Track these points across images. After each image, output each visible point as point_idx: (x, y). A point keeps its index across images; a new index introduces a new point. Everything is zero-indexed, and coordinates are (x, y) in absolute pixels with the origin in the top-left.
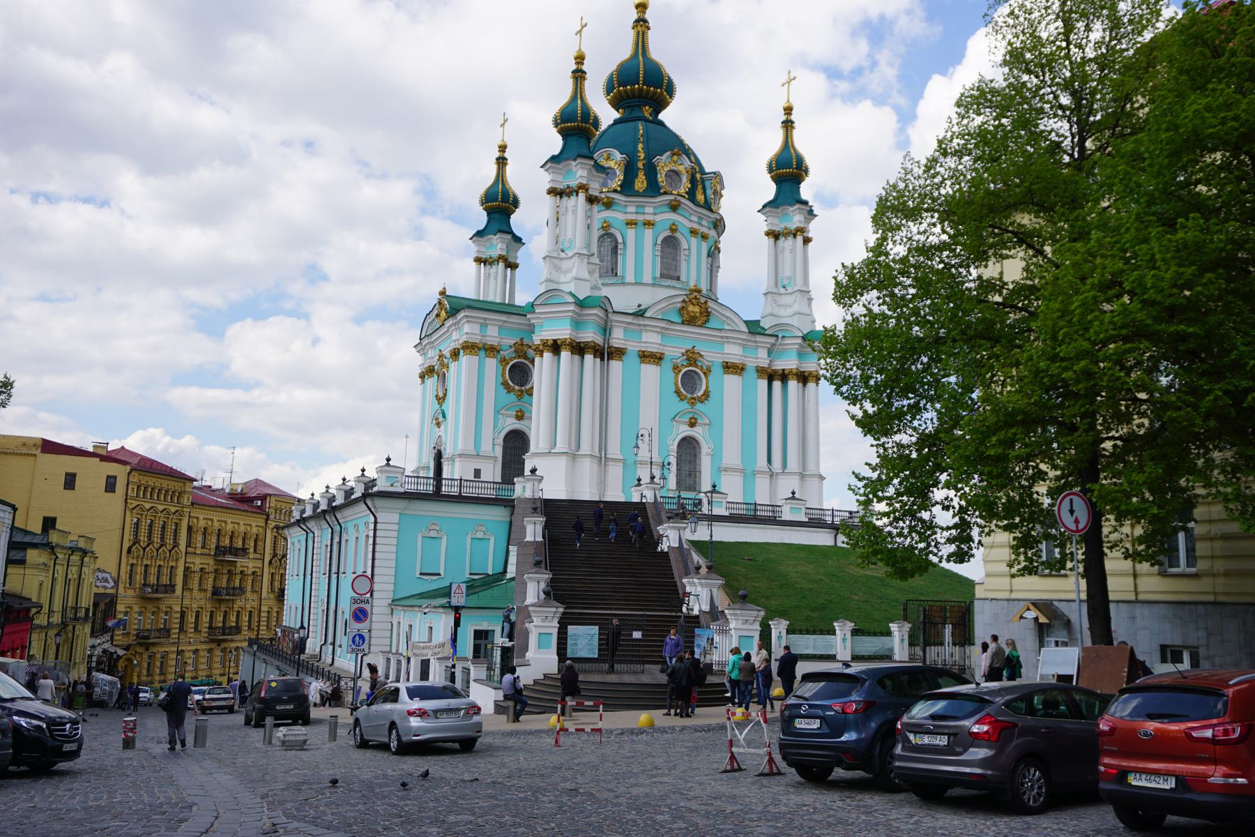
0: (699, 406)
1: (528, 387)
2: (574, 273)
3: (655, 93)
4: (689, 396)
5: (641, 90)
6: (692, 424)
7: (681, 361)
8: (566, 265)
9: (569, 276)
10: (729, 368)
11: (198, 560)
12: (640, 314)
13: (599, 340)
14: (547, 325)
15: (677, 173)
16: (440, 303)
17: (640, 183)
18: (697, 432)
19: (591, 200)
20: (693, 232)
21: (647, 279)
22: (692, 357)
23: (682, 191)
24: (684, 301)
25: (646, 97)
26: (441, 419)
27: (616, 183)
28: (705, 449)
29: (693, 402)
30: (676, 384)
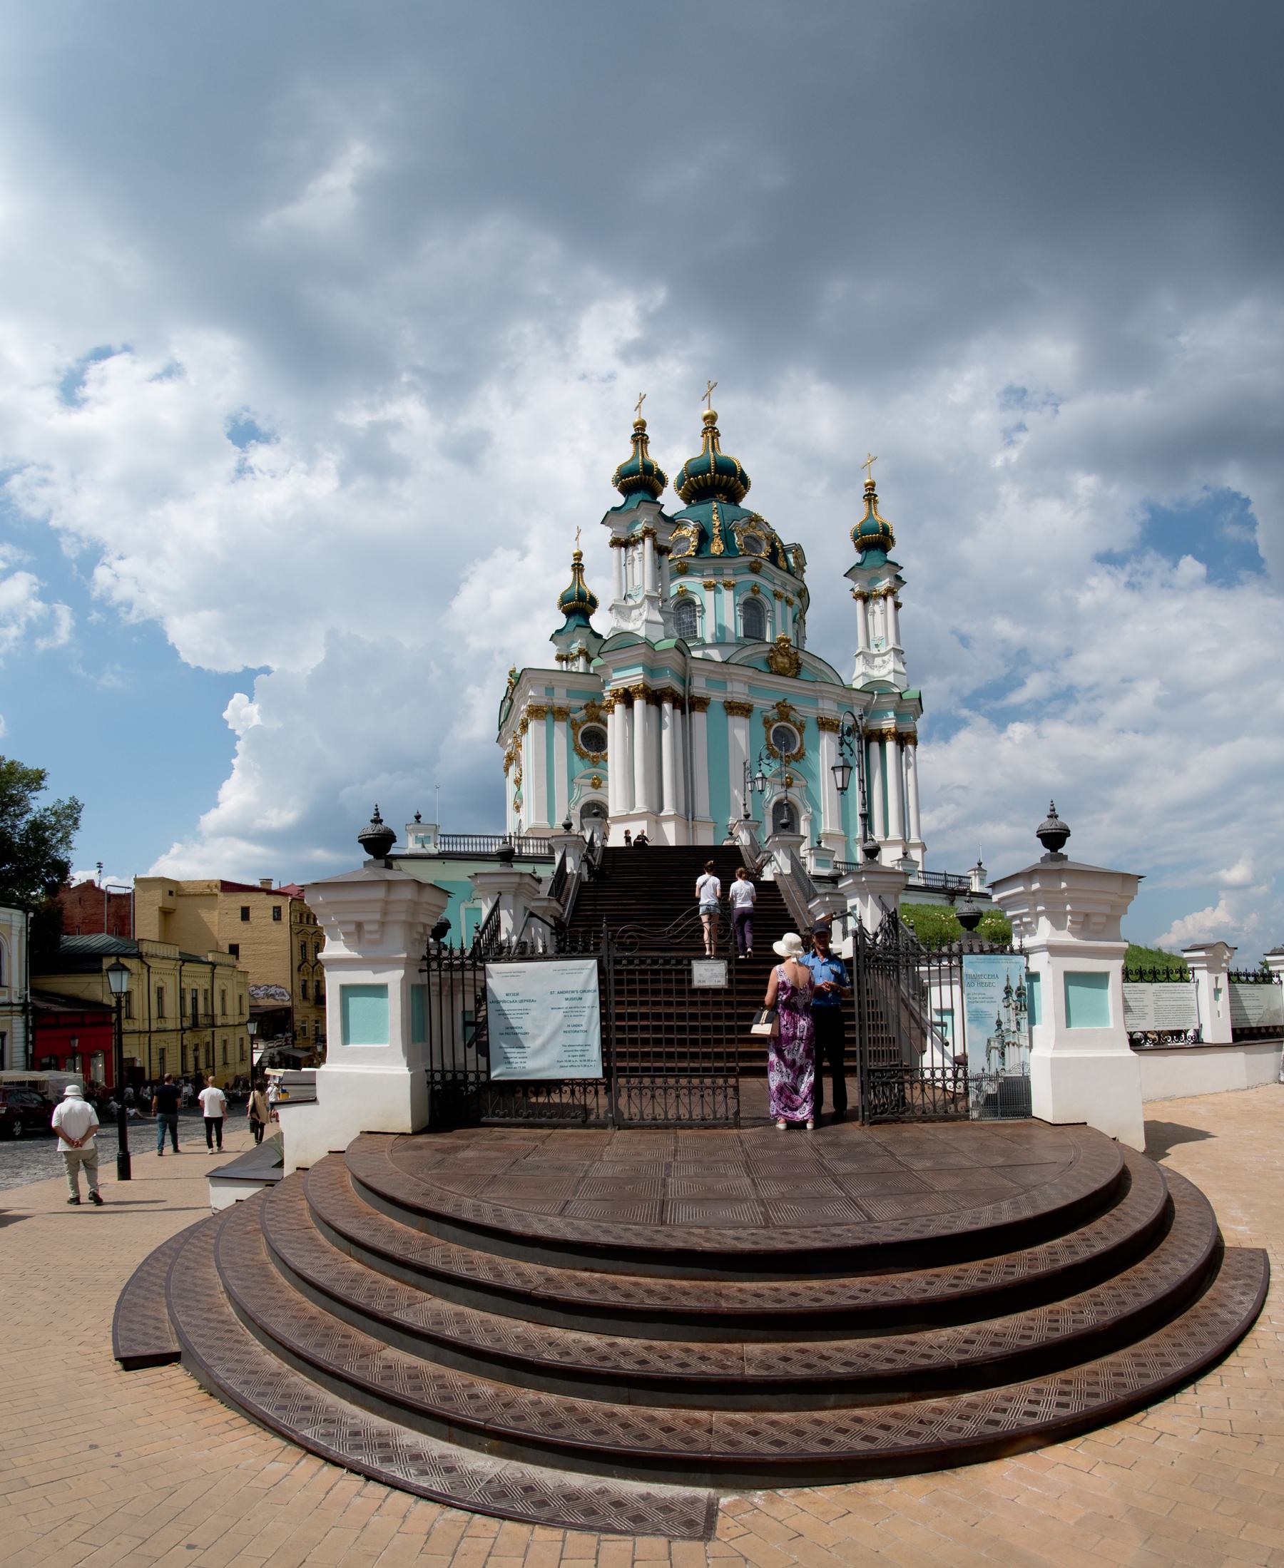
0: (793, 764)
2: (644, 617)
3: (728, 482)
5: (713, 478)
7: (772, 714)
8: (635, 613)
9: (639, 624)
10: (825, 725)
13: (678, 688)
14: (616, 676)
15: (756, 540)
17: (716, 547)
20: (777, 595)
22: (784, 710)
23: (763, 554)
24: (771, 650)
27: (691, 551)
30: (767, 739)
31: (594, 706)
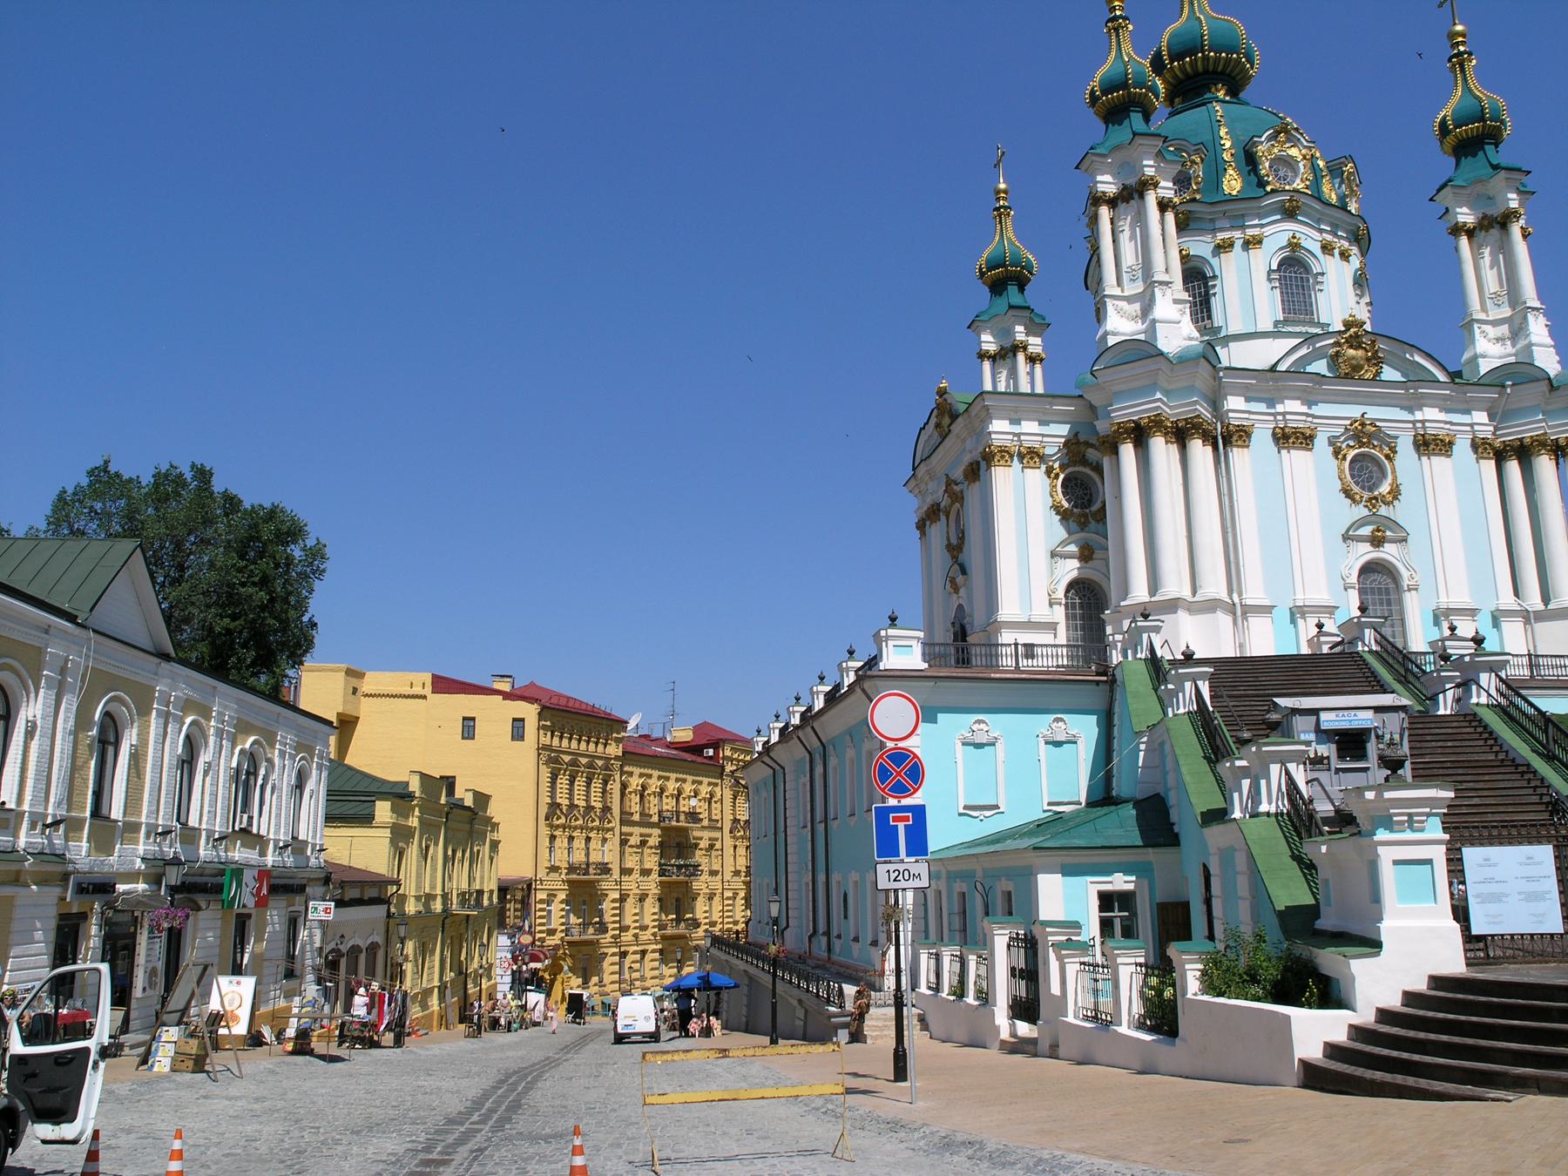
0: (1383, 510)
1: (1095, 508)
3: (1228, 60)
4: (1366, 495)
5: (1206, 58)
6: (1377, 541)
11: (637, 830)
12: (1273, 369)
16: (938, 406)
18: (1389, 552)
19: (1163, 206)
21: (1266, 325)
22: (1362, 433)
23: (1298, 184)
24: (1337, 344)
25: (1215, 72)
26: (960, 579)
28: (1406, 583)
29: (1373, 501)
31: (1078, 443)
